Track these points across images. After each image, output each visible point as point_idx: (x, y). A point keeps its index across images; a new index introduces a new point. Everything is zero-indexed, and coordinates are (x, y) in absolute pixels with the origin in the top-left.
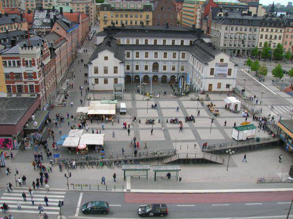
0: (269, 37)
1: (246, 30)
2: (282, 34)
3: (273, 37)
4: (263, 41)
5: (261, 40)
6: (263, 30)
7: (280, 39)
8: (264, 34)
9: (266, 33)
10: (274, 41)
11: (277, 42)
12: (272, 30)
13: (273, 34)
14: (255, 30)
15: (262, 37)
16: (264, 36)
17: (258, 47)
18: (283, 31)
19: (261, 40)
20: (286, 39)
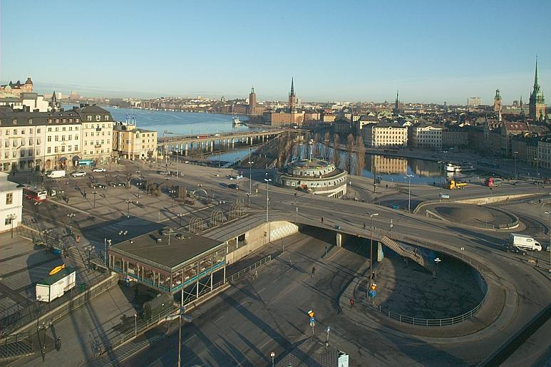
0: (60, 139)
1: (23, 133)
2: (78, 133)
3: (67, 138)
4: (53, 144)
5: (49, 144)
6: (50, 130)
7: (77, 138)
8: (53, 134)
9: (56, 134)
10: (68, 143)
11: (73, 143)
12: (64, 129)
13: (67, 134)
14: (39, 131)
15: (49, 139)
16: (53, 139)
17: (47, 154)
18: (79, 129)
19: (49, 144)
20: (85, 139)
